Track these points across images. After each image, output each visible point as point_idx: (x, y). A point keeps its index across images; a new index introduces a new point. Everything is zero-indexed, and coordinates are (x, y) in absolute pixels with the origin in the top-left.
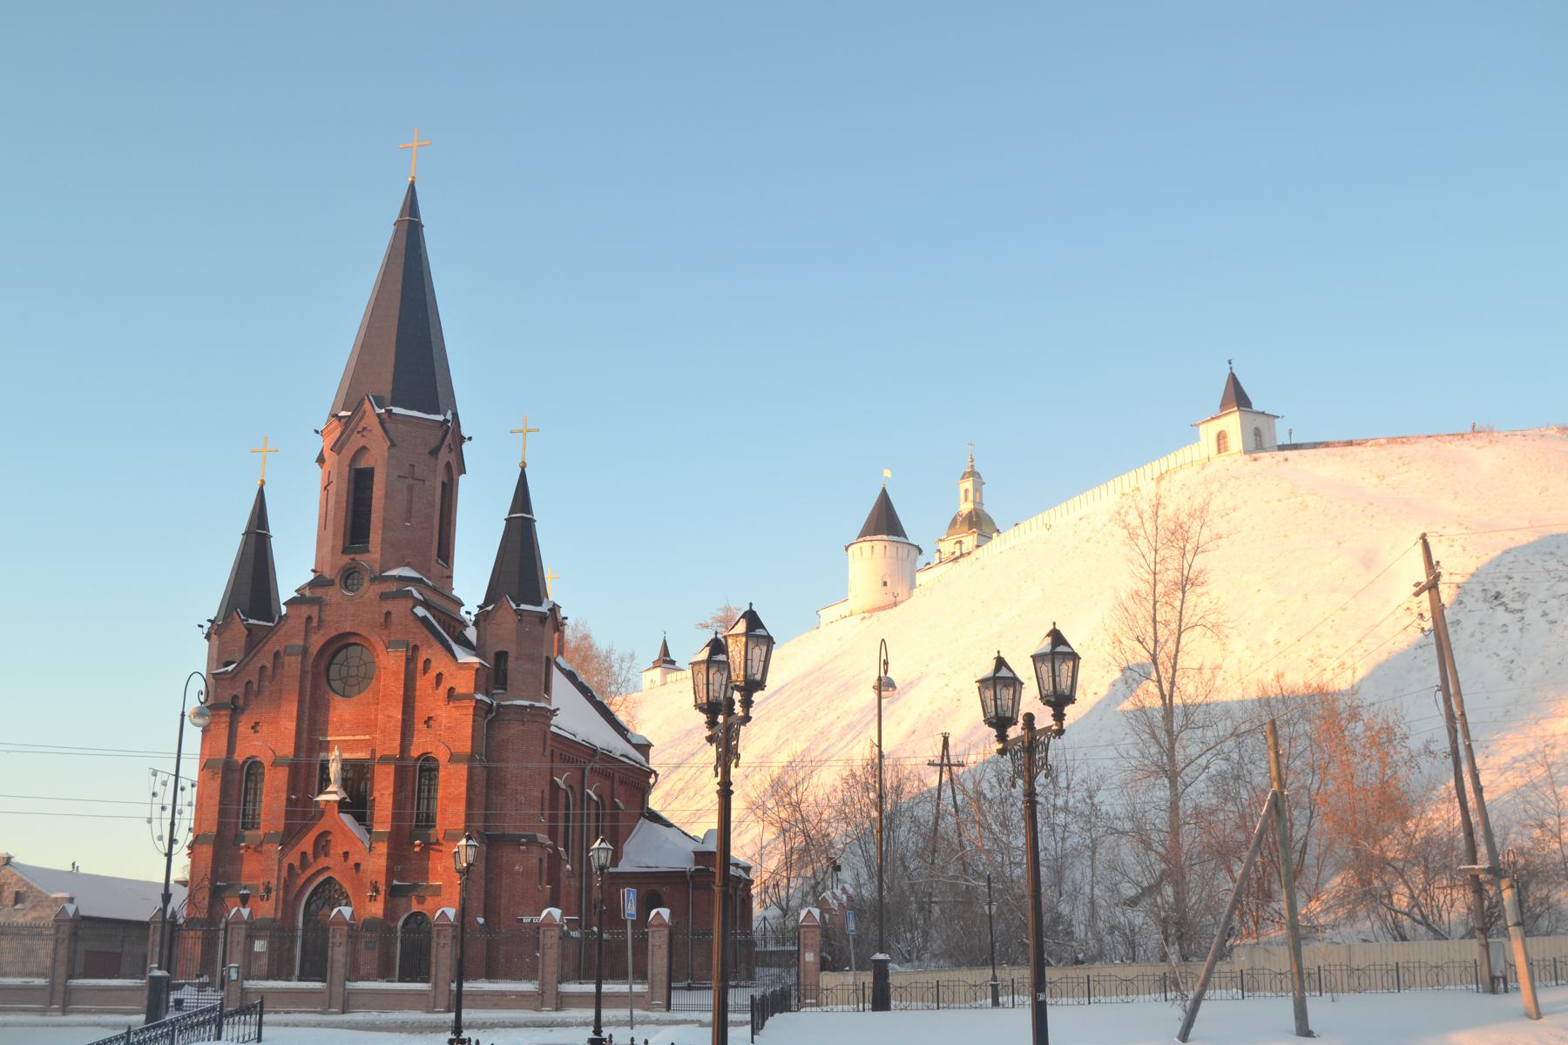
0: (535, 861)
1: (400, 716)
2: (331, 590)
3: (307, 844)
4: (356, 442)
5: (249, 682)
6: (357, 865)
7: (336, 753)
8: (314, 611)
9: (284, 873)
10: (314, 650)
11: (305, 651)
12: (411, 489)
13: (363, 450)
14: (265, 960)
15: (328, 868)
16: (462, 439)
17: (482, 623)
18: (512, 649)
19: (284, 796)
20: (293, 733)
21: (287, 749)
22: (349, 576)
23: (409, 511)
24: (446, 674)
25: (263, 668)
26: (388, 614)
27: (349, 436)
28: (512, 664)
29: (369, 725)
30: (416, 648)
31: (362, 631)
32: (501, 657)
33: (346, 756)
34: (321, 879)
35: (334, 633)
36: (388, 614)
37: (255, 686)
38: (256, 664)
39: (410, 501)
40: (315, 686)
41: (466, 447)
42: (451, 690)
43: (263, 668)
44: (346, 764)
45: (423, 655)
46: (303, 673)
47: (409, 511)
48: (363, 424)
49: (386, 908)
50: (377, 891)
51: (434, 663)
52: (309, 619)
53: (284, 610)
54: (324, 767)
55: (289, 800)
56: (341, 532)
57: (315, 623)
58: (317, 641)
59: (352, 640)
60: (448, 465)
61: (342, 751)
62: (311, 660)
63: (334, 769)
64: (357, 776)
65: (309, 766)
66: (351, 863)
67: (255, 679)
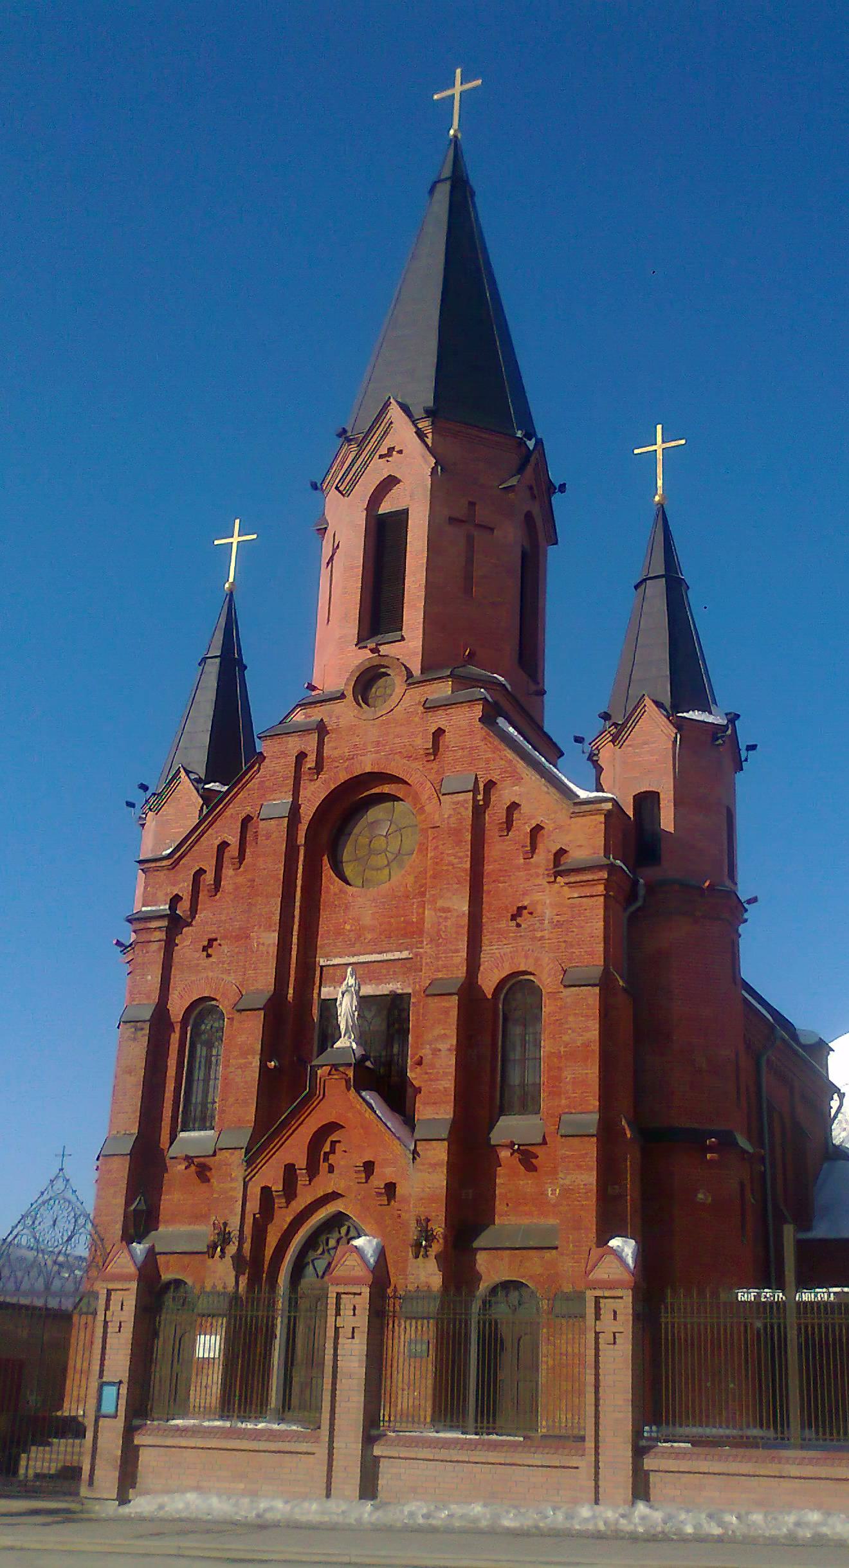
1: (466, 908)
2: (338, 707)
3: (294, 1149)
4: (378, 471)
5: (201, 872)
9: (253, 1206)
10: (307, 812)
11: (295, 808)
12: (470, 540)
13: (390, 482)
14: (214, 1378)
15: (334, 1196)
16: (551, 489)
19: (256, 1062)
20: (273, 950)
21: (263, 981)
23: (468, 578)
24: (549, 826)
25: (224, 845)
26: (439, 733)
27: (366, 465)
29: (411, 932)
30: (490, 785)
33: (367, 990)
34: (322, 1214)
35: (343, 777)
36: (439, 733)
38: (211, 840)
39: (470, 561)
41: (556, 499)
42: (561, 852)
44: (364, 1002)
45: (506, 794)
47: (468, 578)
48: (388, 443)
51: (525, 808)
52: (301, 756)
54: (329, 1007)
55: (263, 1066)
57: (310, 762)
58: (314, 794)
60: (529, 516)
62: (303, 827)
63: (346, 1008)
64: (390, 1016)
66: (378, 1182)
67: (210, 867)
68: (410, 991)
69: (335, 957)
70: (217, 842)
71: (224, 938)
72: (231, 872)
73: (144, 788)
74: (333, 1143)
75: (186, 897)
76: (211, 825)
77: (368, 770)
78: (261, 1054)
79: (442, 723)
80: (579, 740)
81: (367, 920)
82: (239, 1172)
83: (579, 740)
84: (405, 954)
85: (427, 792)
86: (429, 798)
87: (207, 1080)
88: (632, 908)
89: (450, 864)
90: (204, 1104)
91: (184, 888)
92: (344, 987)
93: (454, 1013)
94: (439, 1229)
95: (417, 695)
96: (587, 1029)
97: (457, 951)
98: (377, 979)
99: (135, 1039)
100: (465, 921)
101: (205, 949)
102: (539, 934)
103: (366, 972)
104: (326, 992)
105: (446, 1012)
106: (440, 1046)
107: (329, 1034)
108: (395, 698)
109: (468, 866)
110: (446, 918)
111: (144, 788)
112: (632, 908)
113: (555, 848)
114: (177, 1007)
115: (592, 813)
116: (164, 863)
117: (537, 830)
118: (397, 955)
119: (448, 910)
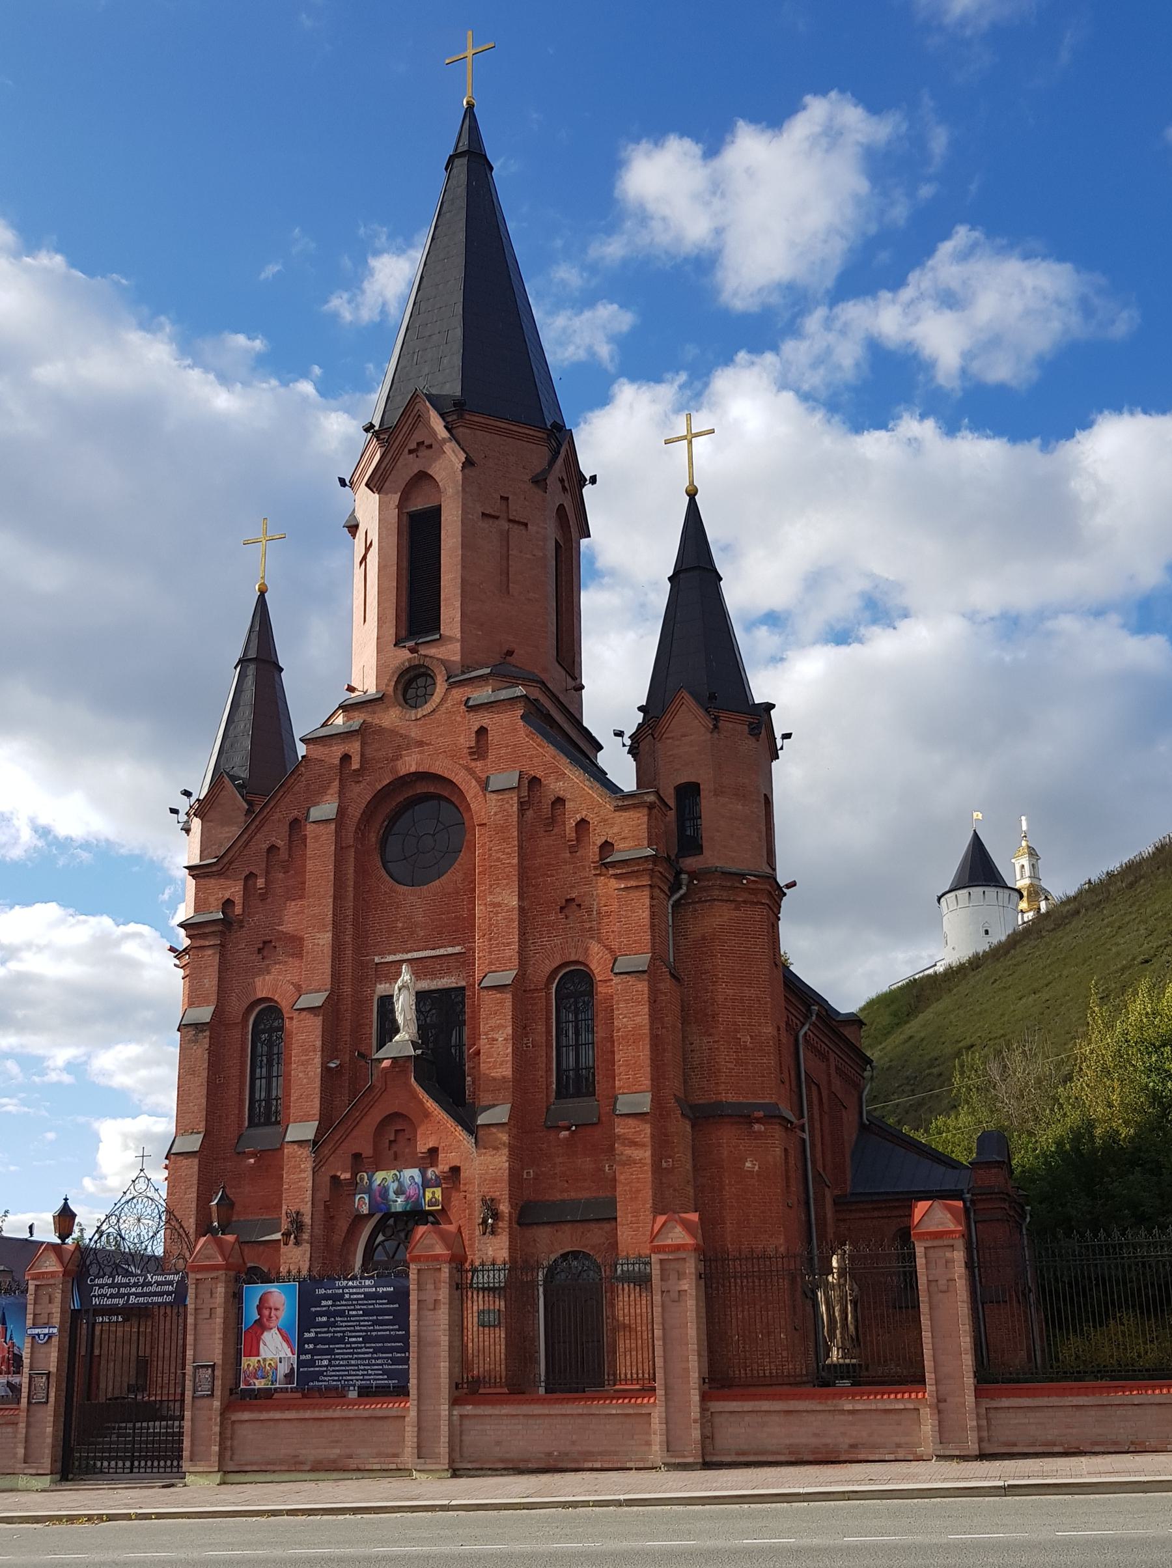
0: (779, 1151)
1: (515, 902)
6: (455, 1170)
7: (406, 976)
8: (354, 748)
9: (324, 1194)
10: (355, 811)
11: (341, 811)
17: (644, 746)
18: (703, 776)
19: (318, 1060)
20: (328, 951)
22: (410, 684)
24: (593, 819)
25: (272, 848)
26: (482, 731)
28: (708, 804)
31: (440, 767)
32: (689, 793)
33: (424, 985)
36: (482, 731)
37: (261, 883)
40: (362, 871)
42: (607, 846)
43: (272, 848)
44: (421, 996)
46: (340, 850)
49: (512, 1249)
50: (496, 1216)
52: (346, 758)
53: (302, 750)
54: (387, 1003)
56: (391, 614)
58: (362, 793)
59: (421, 788)
61: (417, 975)
65: (361, 1004)
68: (463, 984)
69: (390, 954)
70: (265, 846)
71: (279, 939)
72: (281, 875)
73: (187, 794)
74: (397, 1131)
75: (238, 900)
76: (258, 829)
77: (413, 770)
78: (323, 1051)
79: (485, 722)
80: (619, 734)
81: (420, 918)
82: (308, 1165)
83: (619, 734)
84: (457, 949)
85: (471, 789)
86: (475, 797)
87: (269, 1078)
88: (676, 896)
89: (498, 860)
90: (268, 1100)
91: (234, 890)
92: (399, 983)
93: (509, 1004)
94: (504, 1208)
95: (458, 694)
96: (637, 1014)
97: (509, 944)
98: (433, 975)
99: (196, 1041)
100: (515, 915)
101: (260, 950)
102: (587, 925)
103: (420, 968)
104: (382, 989)
105: (501, 1003)
106: (496, 1036)
107: (389, 1028)
108: (436, 698)
109: (515, 861)
110: (497, 913)
111: (187, 794)
112: (676, 896)
113: (599, 843)
114: (236, 1007)
115: (635, 807)
116: (214, 869)
117: (583, 824)
118: (450, 950)
119: (499, 905)
